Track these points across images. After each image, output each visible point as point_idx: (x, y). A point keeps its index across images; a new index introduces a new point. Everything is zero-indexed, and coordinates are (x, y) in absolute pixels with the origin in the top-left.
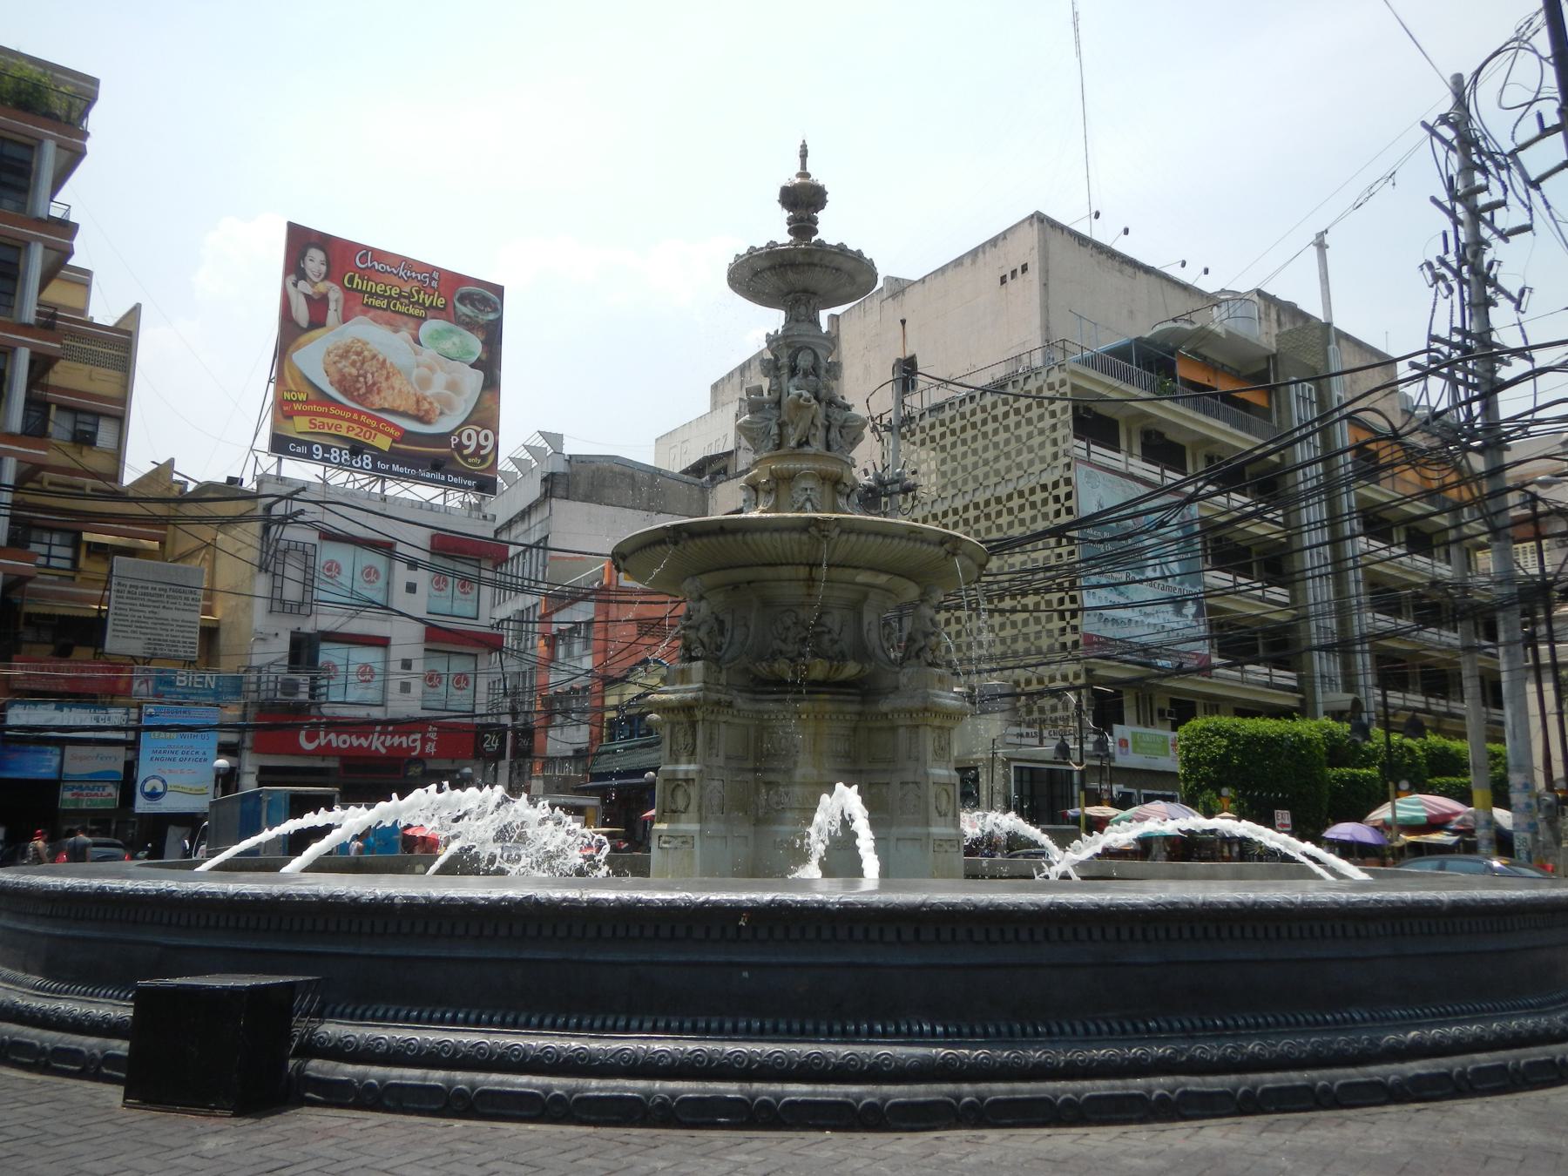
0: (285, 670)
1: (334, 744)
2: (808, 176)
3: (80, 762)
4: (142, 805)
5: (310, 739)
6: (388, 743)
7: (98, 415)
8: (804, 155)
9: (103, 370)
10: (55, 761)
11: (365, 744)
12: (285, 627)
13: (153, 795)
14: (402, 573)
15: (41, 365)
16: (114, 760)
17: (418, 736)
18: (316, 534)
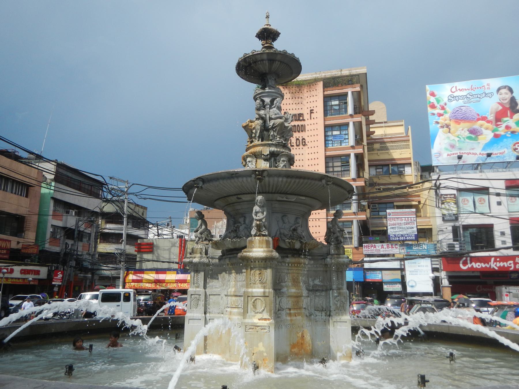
0: (452, 241)
1: (475, 267)
2: (270, 25)
3: (387, 276)
4: (409, 290)
5: (464, 265)
6: (498, 265)
7: (404, 165)
8: (268, 17)
9: (402, 150)
10: (380, 276)
11: (488, 266)
12: (449, 226)
13: (412, 286)
14: (494, 199)
15: (359, 158)
16: (397, 275)
17: (512, 262)
18: (456, 191)
